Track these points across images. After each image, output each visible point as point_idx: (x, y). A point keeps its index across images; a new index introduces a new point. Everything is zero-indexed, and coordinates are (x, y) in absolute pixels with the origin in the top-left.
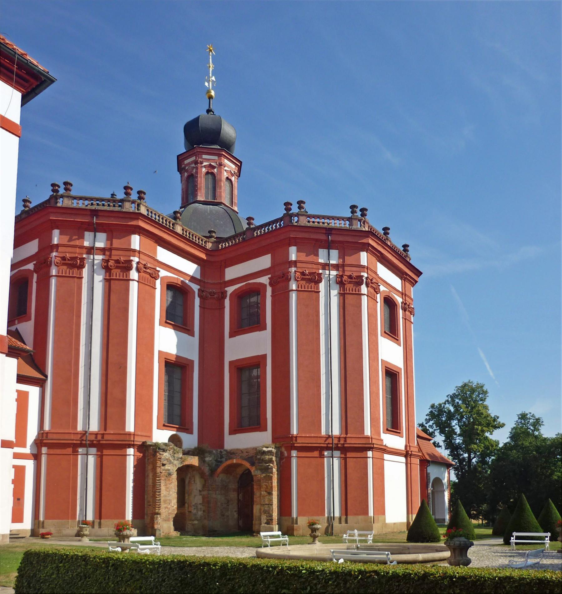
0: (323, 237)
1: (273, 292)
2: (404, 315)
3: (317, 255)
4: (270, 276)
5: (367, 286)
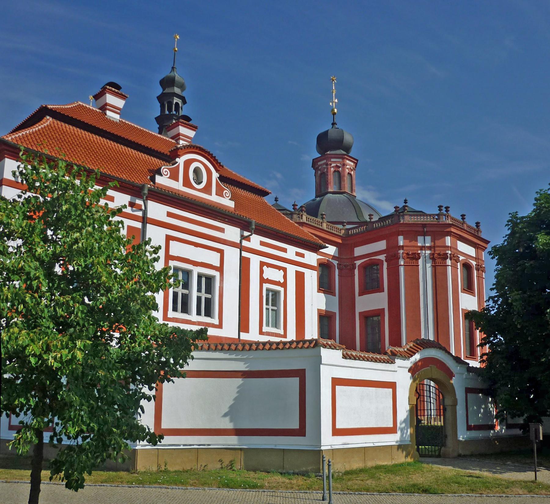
0: (421, 229)
1: (388, 266)
2: (478, 274)
3: (417, 241)
4: (385, 255)
5: (451, 259)
